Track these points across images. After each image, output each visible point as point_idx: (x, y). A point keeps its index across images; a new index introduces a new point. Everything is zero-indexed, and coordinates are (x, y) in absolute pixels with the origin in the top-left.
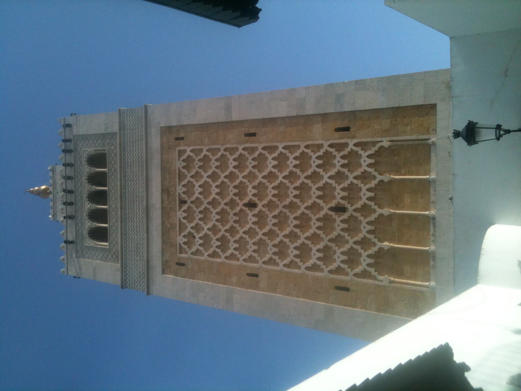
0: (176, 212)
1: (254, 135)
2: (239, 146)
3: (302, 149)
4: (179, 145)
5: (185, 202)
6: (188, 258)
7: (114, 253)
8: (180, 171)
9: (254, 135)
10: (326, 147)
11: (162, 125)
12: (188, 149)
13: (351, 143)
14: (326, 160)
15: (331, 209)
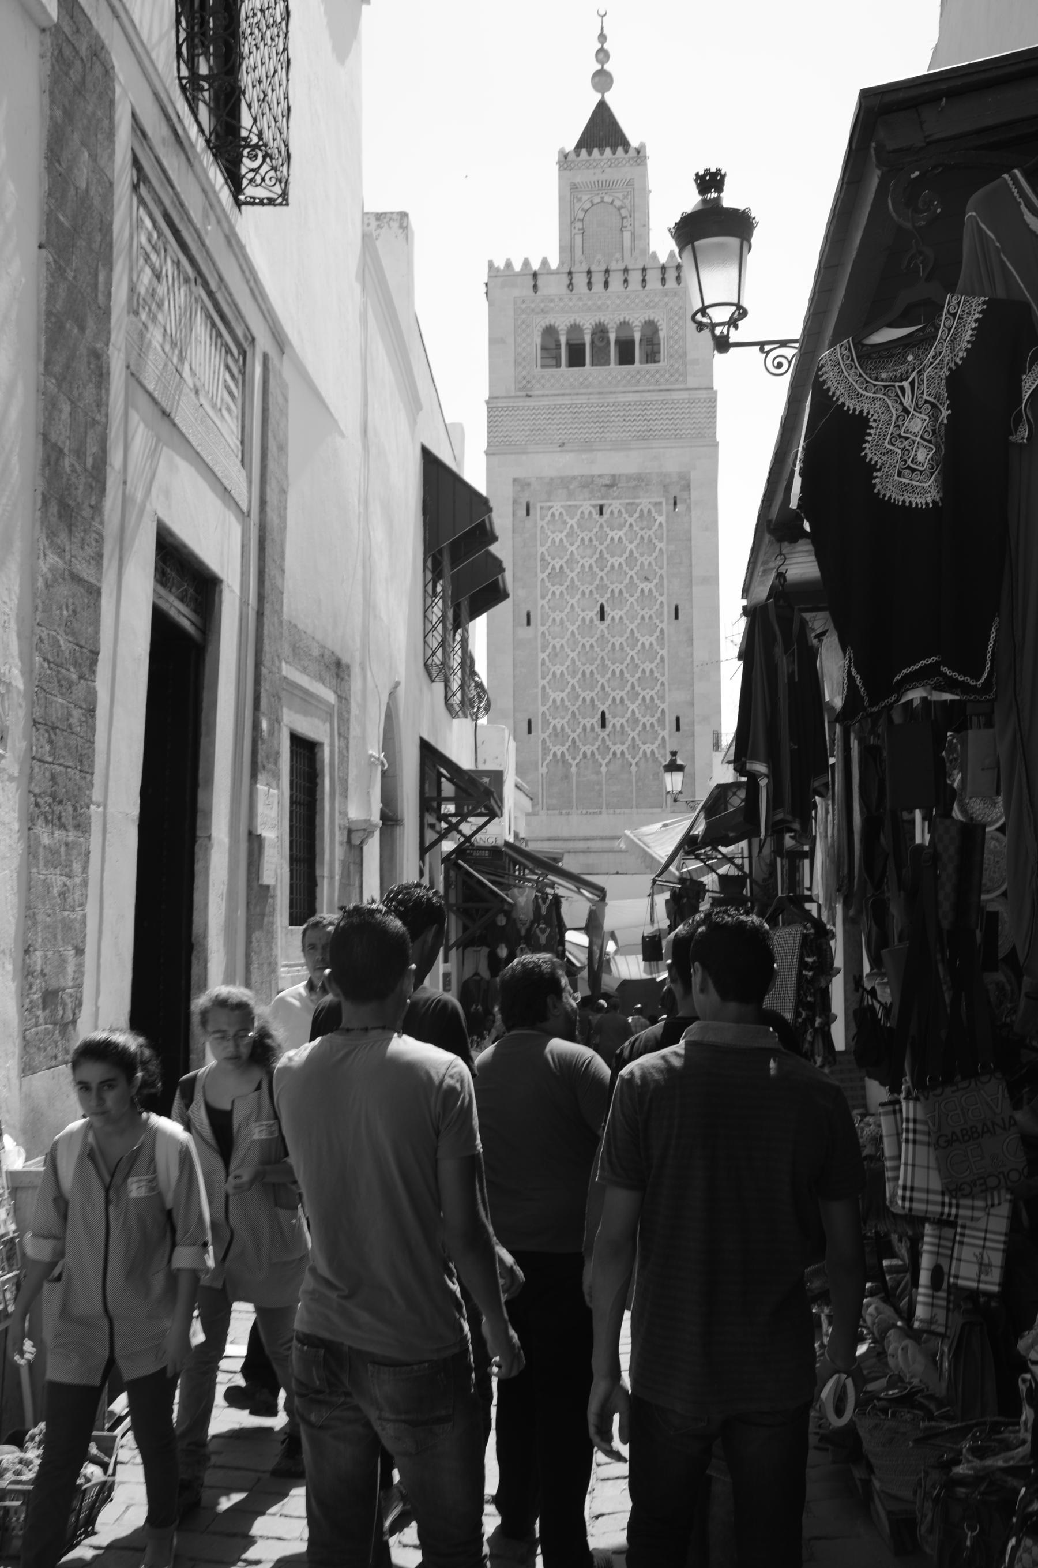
0: (590, 499)
1: (677, 617)
2: (665, 596)
3: (661, 679)
4: (667, 504)
5: (601, 513)
6: (536, 523)
7: (529, 382)
8: (638, 505)
9: (677, 617)
10: (662, 706)
11: (695, 476)
12: (662, 519)
13: (665, 733)
14: (649, 706)
15: (603, 714)
